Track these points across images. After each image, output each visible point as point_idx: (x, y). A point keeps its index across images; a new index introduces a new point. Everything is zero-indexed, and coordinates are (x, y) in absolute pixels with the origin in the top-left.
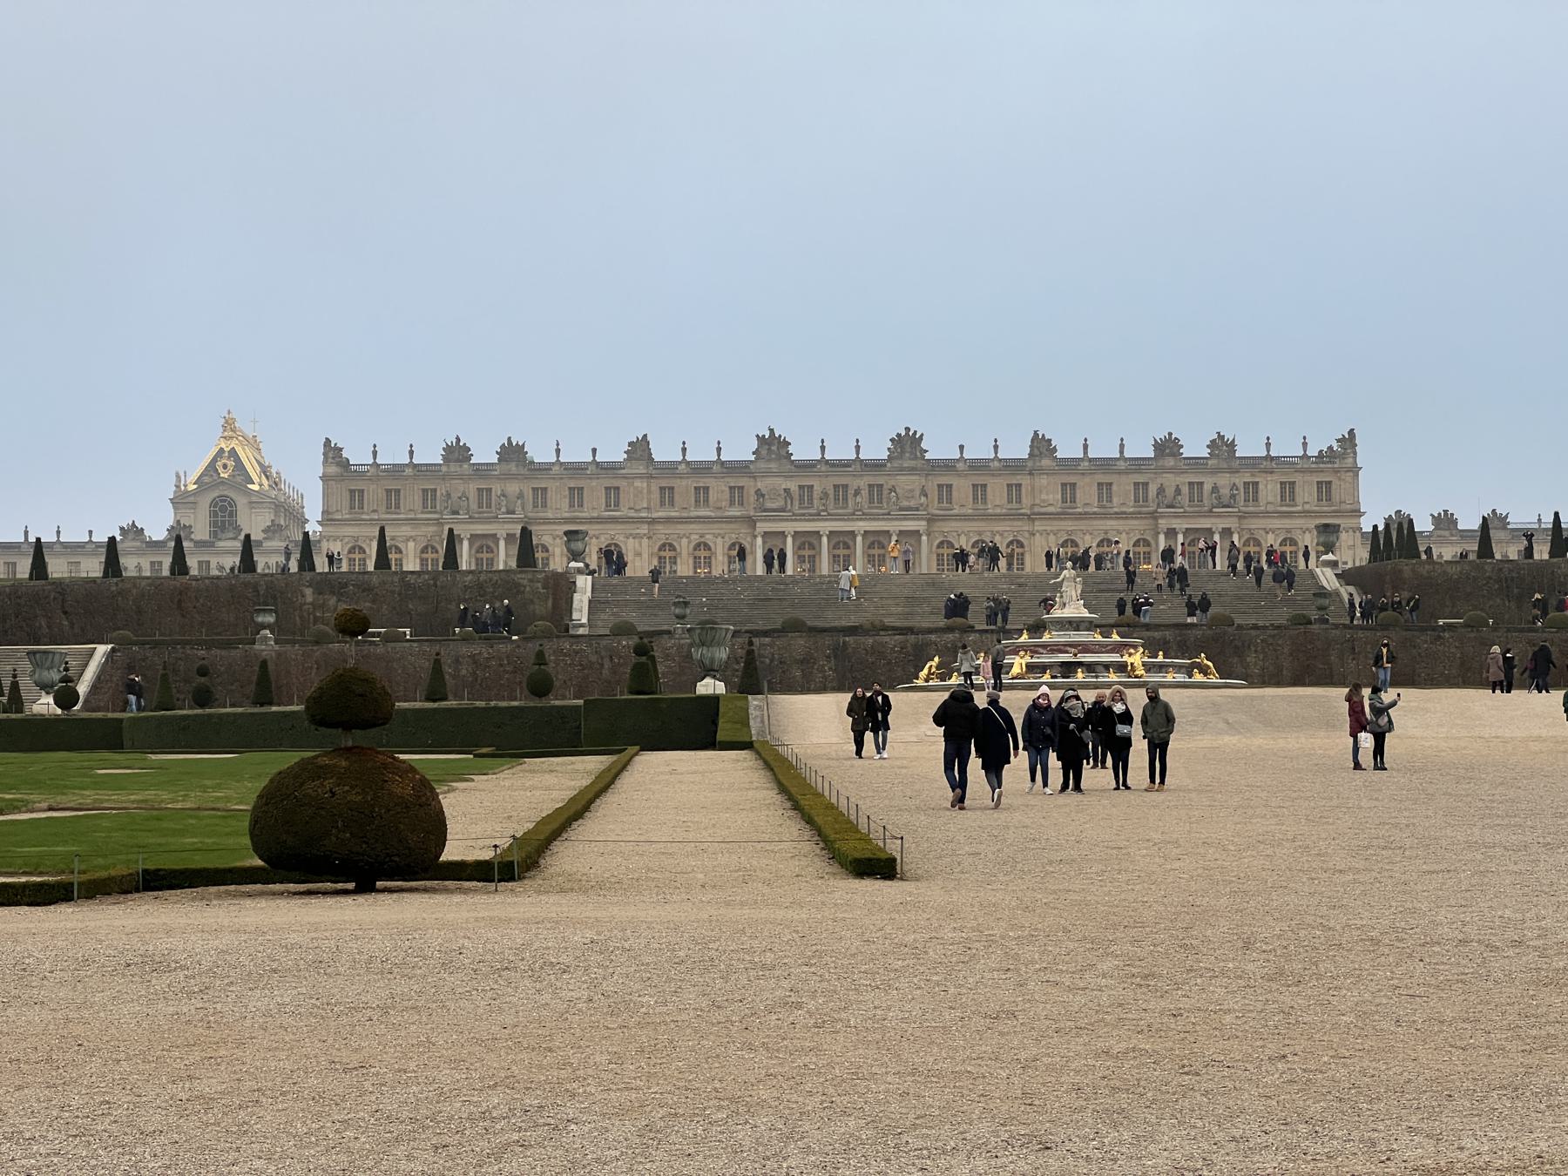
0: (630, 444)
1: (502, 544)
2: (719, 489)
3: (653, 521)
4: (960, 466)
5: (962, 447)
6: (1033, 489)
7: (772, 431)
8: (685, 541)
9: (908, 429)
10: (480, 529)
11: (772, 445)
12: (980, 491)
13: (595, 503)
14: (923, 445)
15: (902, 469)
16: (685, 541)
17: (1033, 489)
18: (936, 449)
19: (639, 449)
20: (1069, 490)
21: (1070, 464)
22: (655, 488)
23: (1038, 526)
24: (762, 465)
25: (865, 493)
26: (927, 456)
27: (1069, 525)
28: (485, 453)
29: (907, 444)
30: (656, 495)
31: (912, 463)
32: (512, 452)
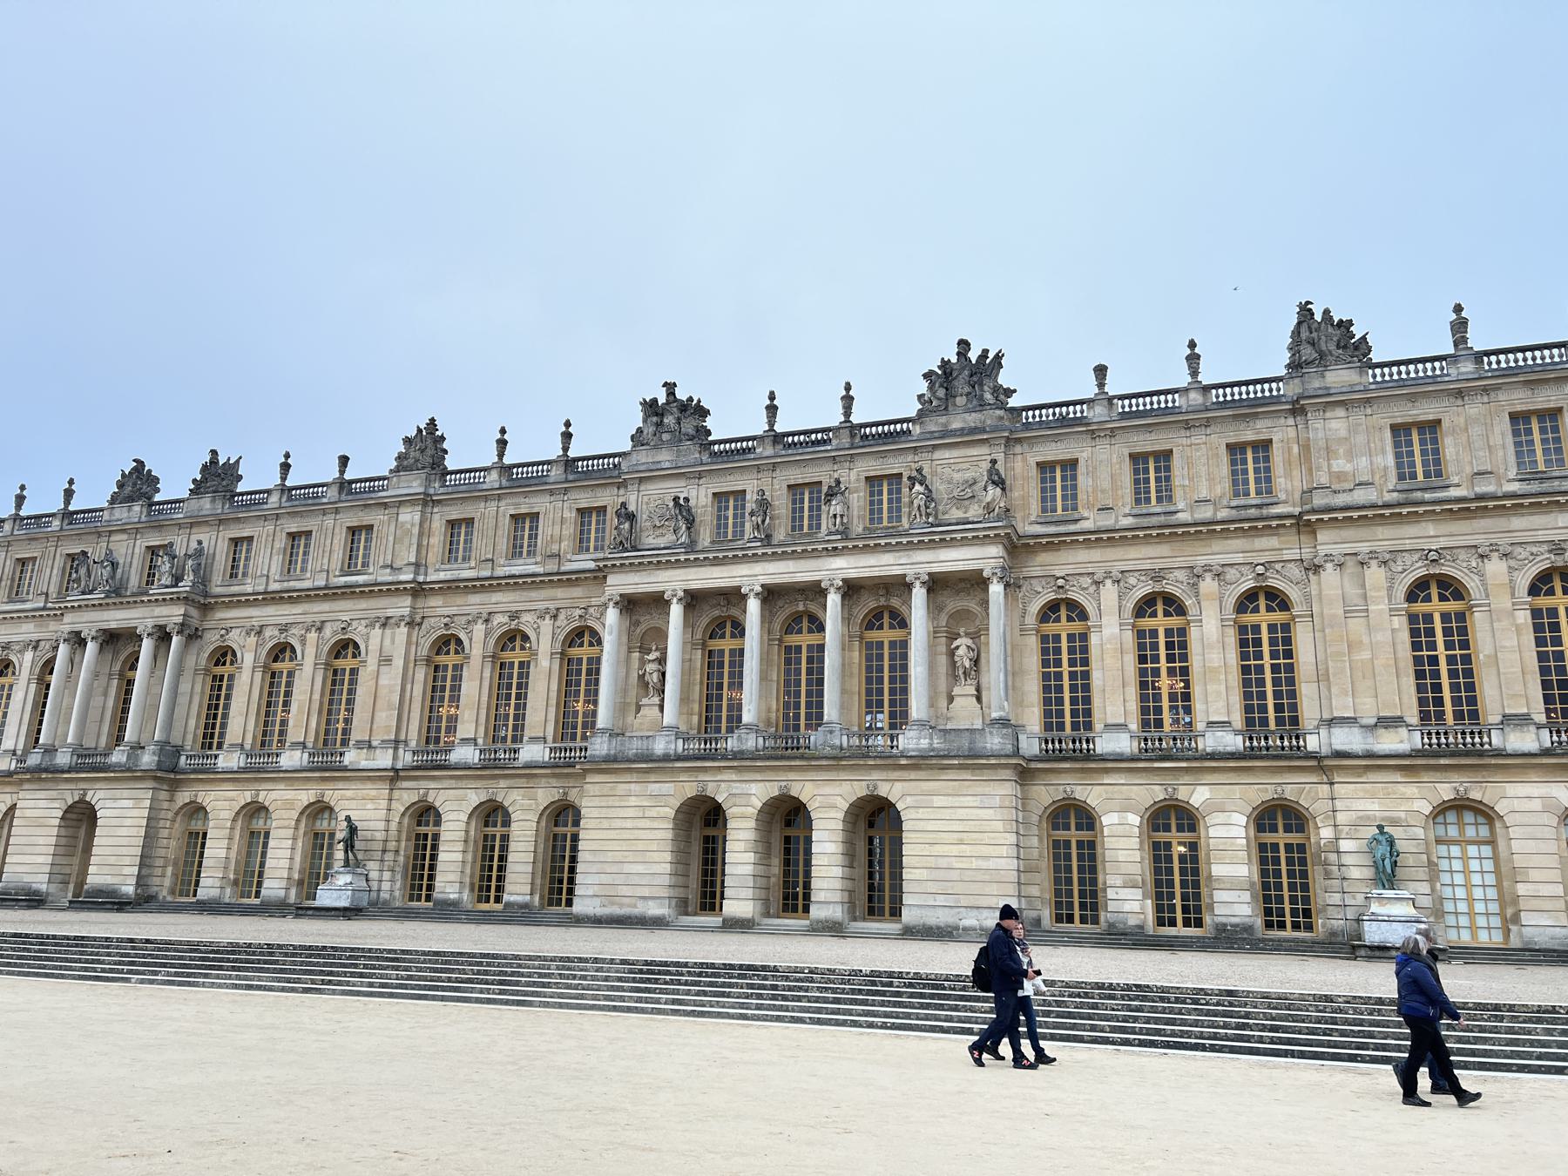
0: (408, 441)
1: (147, 646)
2: (557, 517)
3: (419, 591)
4: (1098, 413)
5: (1101, 371)
6: (1306, 448)
7: (670, 387)
8: (479, 629)
9: (964, 345)
10: (116, 618)
11: (674, 418)
12: (1152, 469)
13: (326, 558)
14: (1004, 379)
15: (945, 433)
16: (479, 629)
17: (1306, 448)
18: (1031, 382)
19: (426, 448)
20: (1417, 439)
21: (1415, 380)
22: (438, 524)
23: (1329, 542)
24: (644, 457)
25: (858, 500)
26: (1013, 402)
27: (1432, 534)
28: (175, 484)
29: (966, 378)
30: (437, 540)
31: (972, 419)
32: (218, 477)
